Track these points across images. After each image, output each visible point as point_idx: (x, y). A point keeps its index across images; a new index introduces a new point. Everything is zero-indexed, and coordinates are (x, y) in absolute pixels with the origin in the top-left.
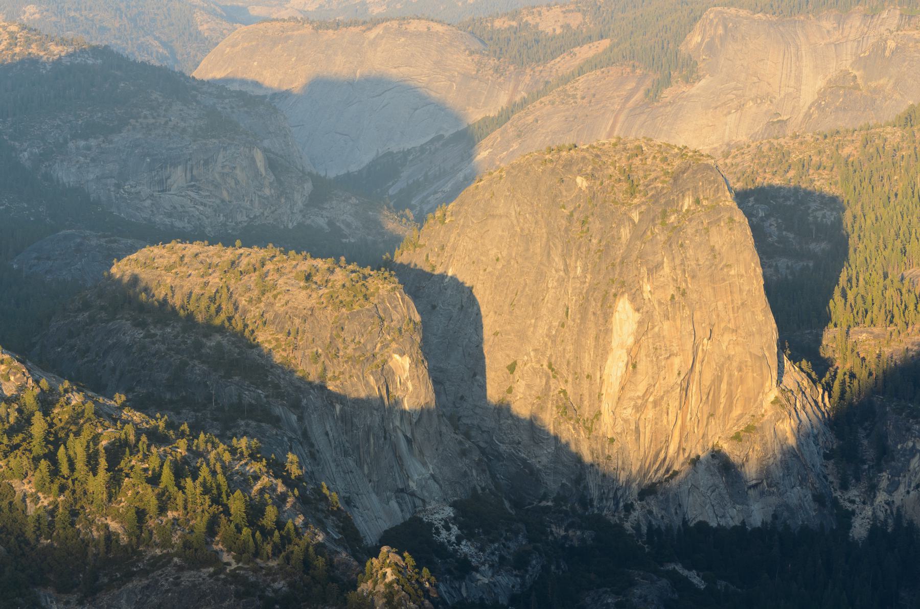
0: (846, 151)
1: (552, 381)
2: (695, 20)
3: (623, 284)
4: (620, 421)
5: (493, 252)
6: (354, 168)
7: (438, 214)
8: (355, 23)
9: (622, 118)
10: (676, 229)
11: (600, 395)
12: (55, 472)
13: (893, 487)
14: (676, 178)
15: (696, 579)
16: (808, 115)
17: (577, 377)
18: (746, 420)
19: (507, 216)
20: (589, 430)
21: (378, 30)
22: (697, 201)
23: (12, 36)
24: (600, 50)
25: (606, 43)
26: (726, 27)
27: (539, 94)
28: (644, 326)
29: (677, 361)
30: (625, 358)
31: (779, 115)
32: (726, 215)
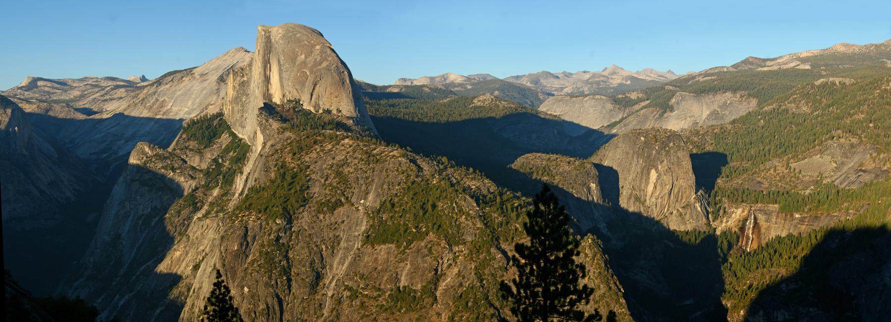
0: (715, 131)
1: (633, 192)
2: (674, 96)
3: (653, 166)
4: (651, 202)
5: (618, 157)
6: (580, 134)
7: (603, 146)
8: (581, 96)
9: (653, 121)
10: (668, 152)
11: (646, 195)
12: (503, 212)
13: (727, 221)
14: (668, 137)
15: (671, 245)
16: (704, 121)
17: (640, 190)
18: (686, 202)
19: (622, 147)
20: (643, 204)
21: (587, 98)
22: (674, 144)
23: (492, 99)
24: (647, 103)
25: (649, 101)
26: (682, 97)
27: (630, 115)
28: (659, 177)
29: (667, 187)
30: (653, 186)
31: (696, 121)
32: (682, 148)
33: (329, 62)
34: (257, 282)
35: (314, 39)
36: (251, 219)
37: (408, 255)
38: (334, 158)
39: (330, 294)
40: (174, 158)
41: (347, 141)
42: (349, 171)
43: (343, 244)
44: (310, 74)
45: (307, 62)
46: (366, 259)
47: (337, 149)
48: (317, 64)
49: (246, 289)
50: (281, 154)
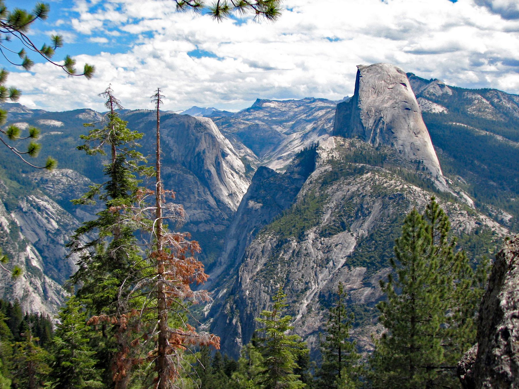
33: (395, 100)
34: (257, 287)
35: (392, 79)
36: (270, 237)
37: (373, 278)
38: (348, 191)
39: (306, 303)
40: (284, 180)
41: (369, 174)
42: (356, 202)
43: (331, 263)
44: (376, 112)
45: (377, 100)
46: (342, 277)
47: (356, 181)
48: (383, 102)
49: (248, 292)
50: (315, 184)
